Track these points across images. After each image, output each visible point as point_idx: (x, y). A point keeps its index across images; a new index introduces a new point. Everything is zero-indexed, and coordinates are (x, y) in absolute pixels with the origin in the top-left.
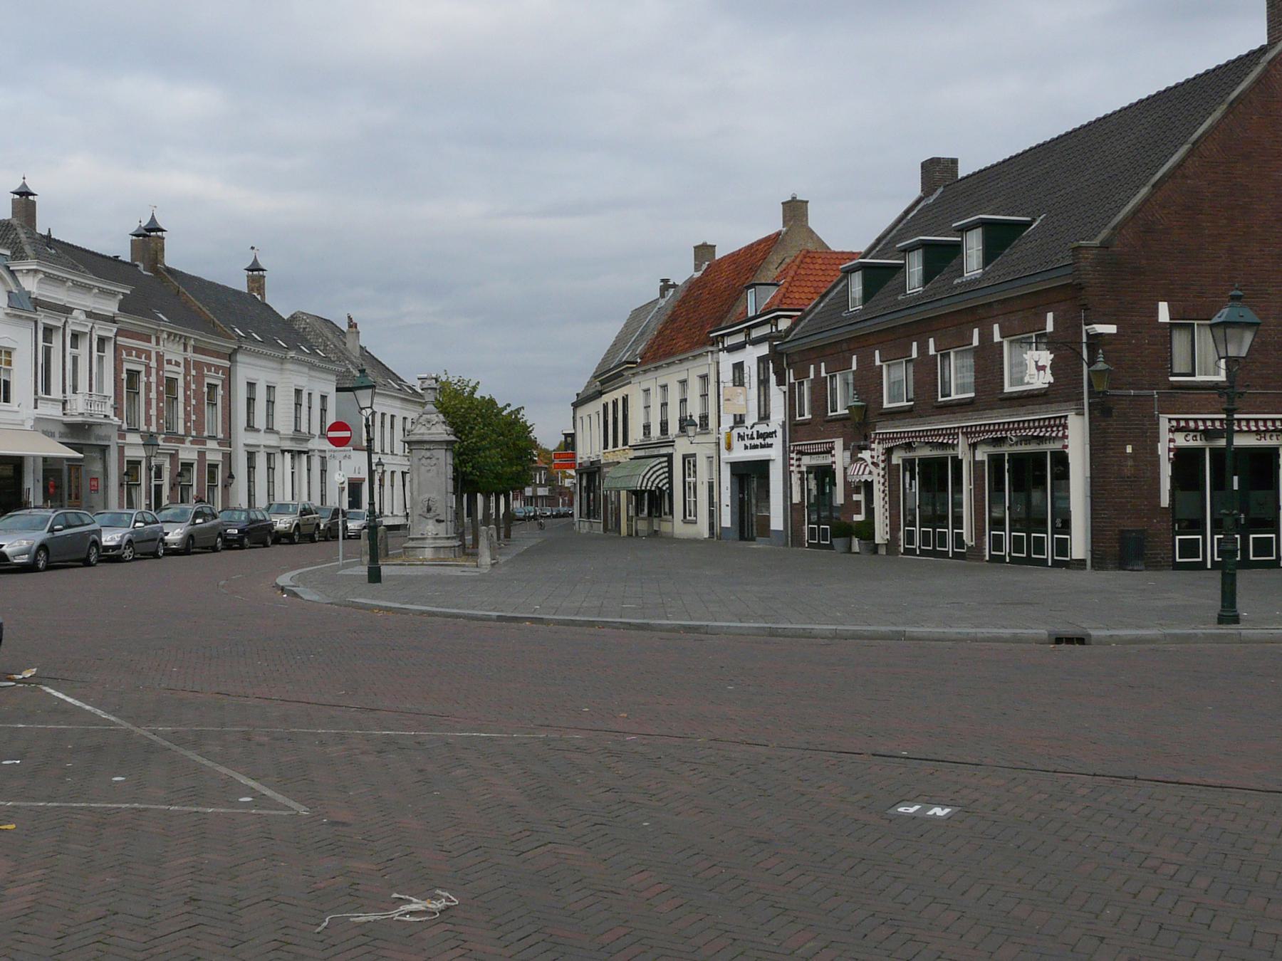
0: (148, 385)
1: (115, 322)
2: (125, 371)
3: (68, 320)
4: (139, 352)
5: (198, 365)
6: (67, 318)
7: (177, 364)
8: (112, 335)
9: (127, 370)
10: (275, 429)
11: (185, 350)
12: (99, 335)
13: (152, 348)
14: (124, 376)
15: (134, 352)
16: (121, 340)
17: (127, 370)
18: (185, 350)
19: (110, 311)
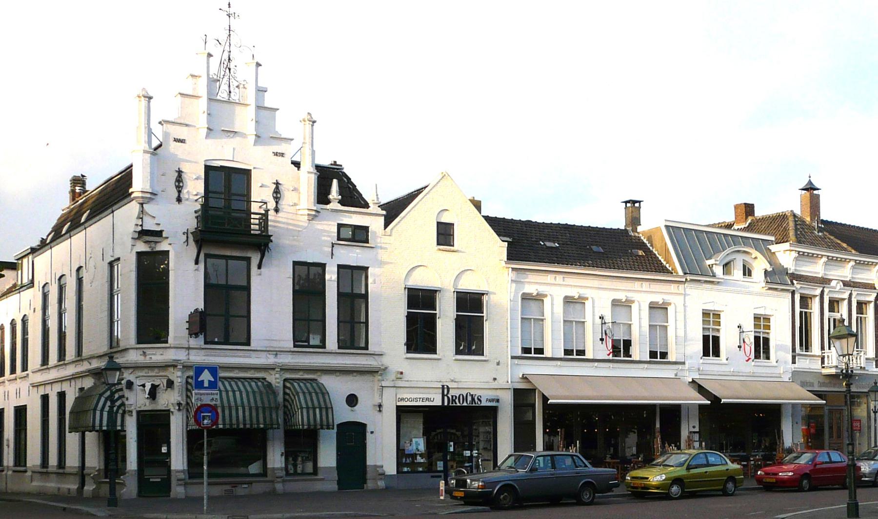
3: (825, 289)
6: (824, 288)
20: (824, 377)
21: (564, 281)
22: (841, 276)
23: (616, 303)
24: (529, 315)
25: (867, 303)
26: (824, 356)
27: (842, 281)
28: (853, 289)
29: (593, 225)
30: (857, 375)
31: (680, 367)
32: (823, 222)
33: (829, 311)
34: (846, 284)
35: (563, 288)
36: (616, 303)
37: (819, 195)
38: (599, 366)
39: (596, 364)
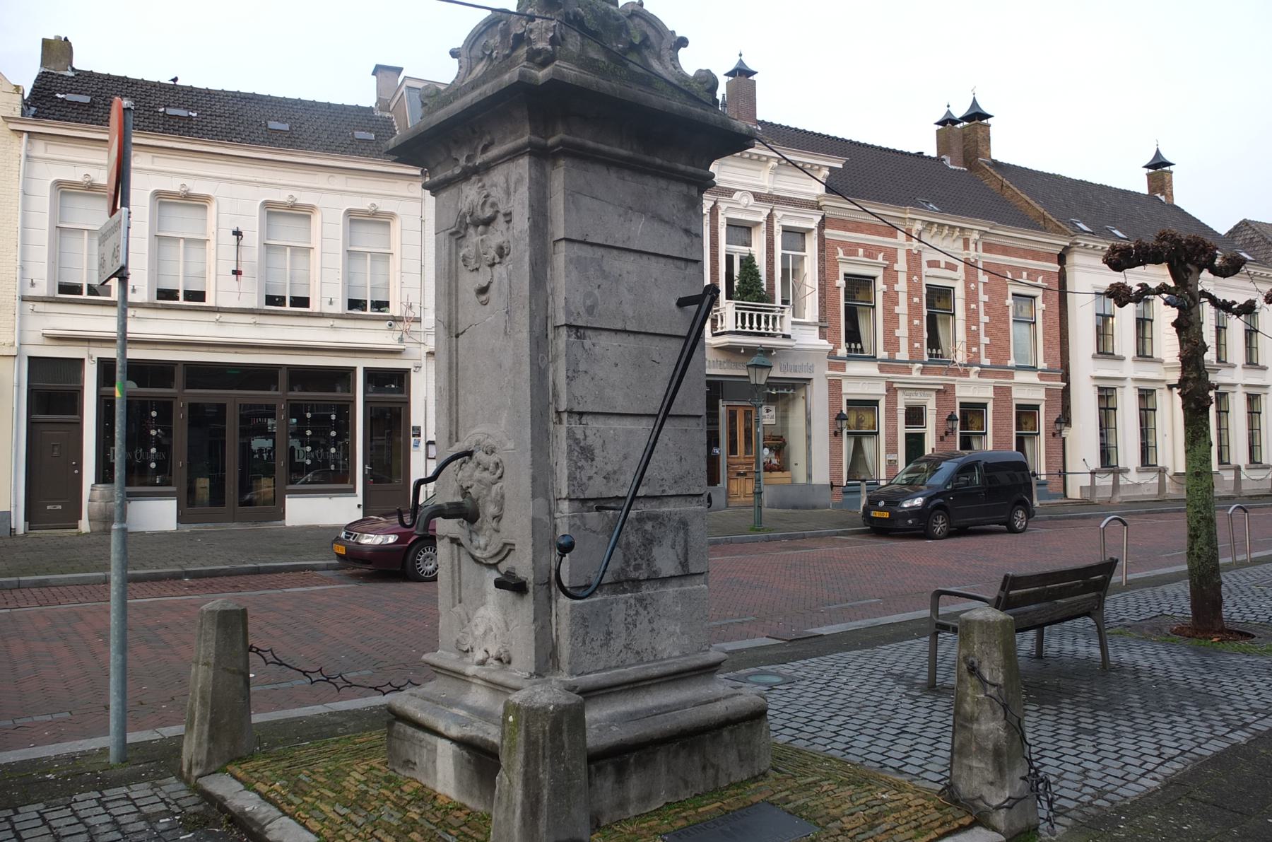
0: (891, 298)
1: (820, 208)
2: (841, 276)
4: (871, 251)
5: (995, 272)
7: (952, 267)
8: (811, 221)
9: (845, 275)
10: (1116, 353)
11: (966, 246)
12: (783, 226)
13: (899, 244)
14: (841, 282)
15: (861, 251)
16: (830, 233)
17: (845, 275)
18: (966, 246)
19: (807, 194)
20: (716, 351)
21: (153, 162)
22: (752, 185)
23: (272, 210)
24: (69, 223)
25: (802, 233)
26: (716, 316)
27: (752, 192)
28: (777, 206)
29: (307, 96)
30: (776, 349)
31: (414, 326)
32: (762, 123)
33: (727, 243)
34: (758, 197)
35: (153, 177)
36: (272, 210)
37: (755, 81)
38: (221, 320)
39: (218, 315)
